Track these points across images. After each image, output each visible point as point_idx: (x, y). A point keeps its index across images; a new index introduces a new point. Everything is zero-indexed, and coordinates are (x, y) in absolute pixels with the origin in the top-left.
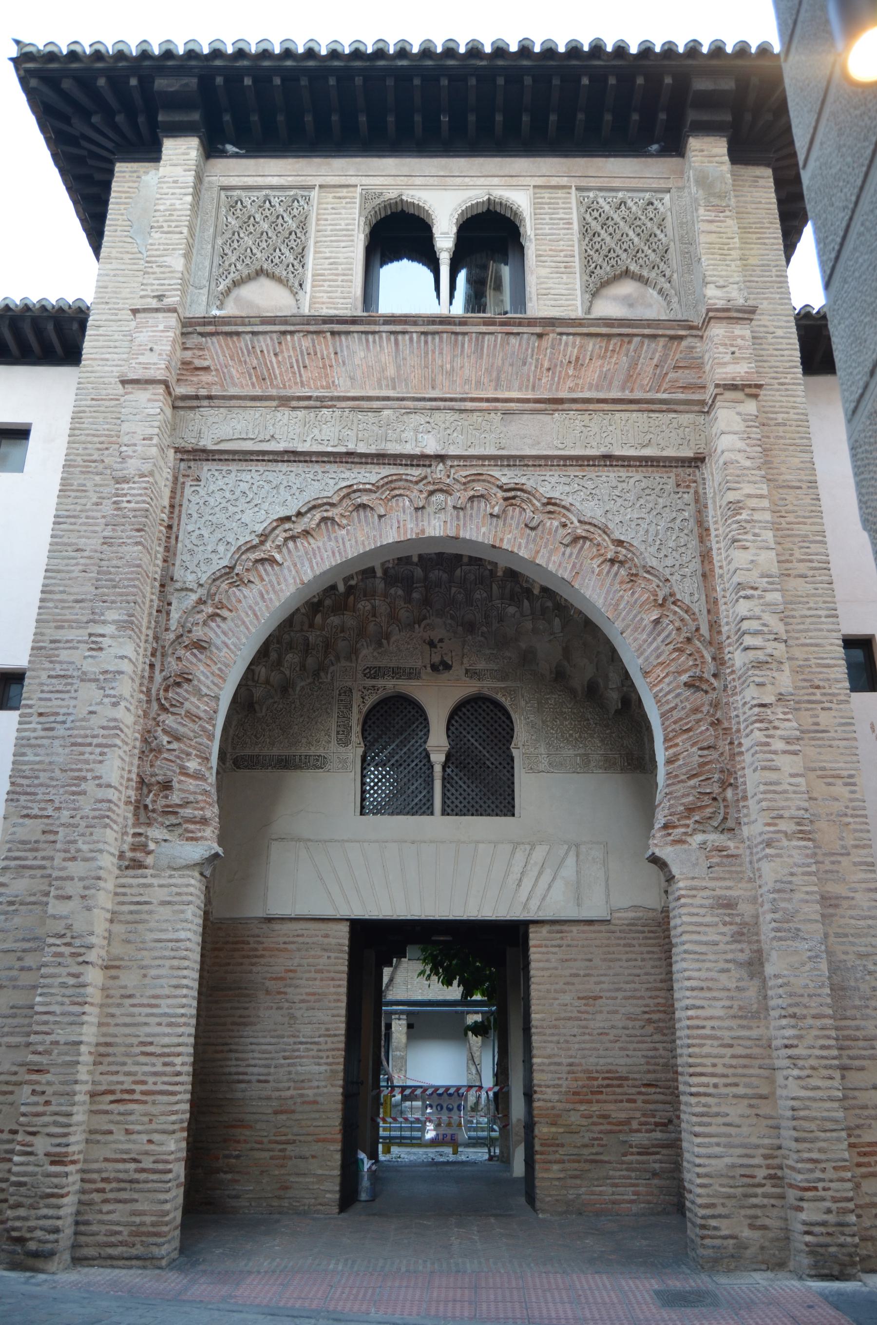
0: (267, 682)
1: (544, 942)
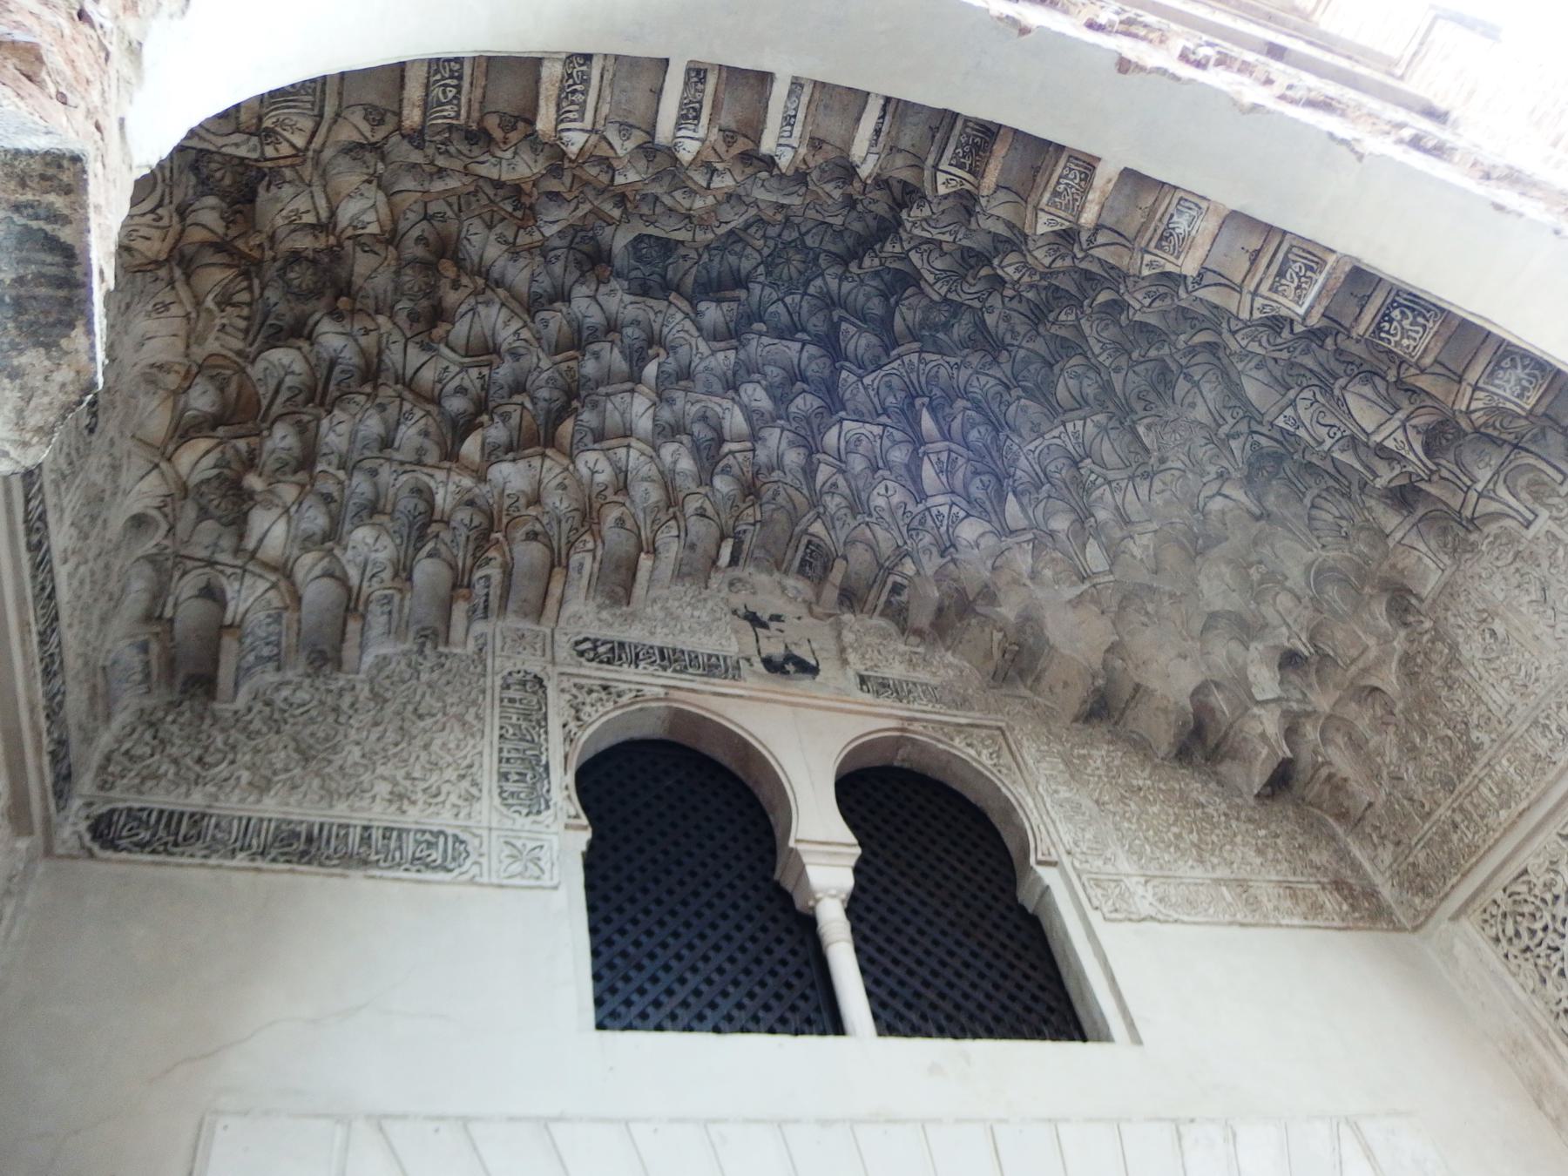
0: (284, 570)
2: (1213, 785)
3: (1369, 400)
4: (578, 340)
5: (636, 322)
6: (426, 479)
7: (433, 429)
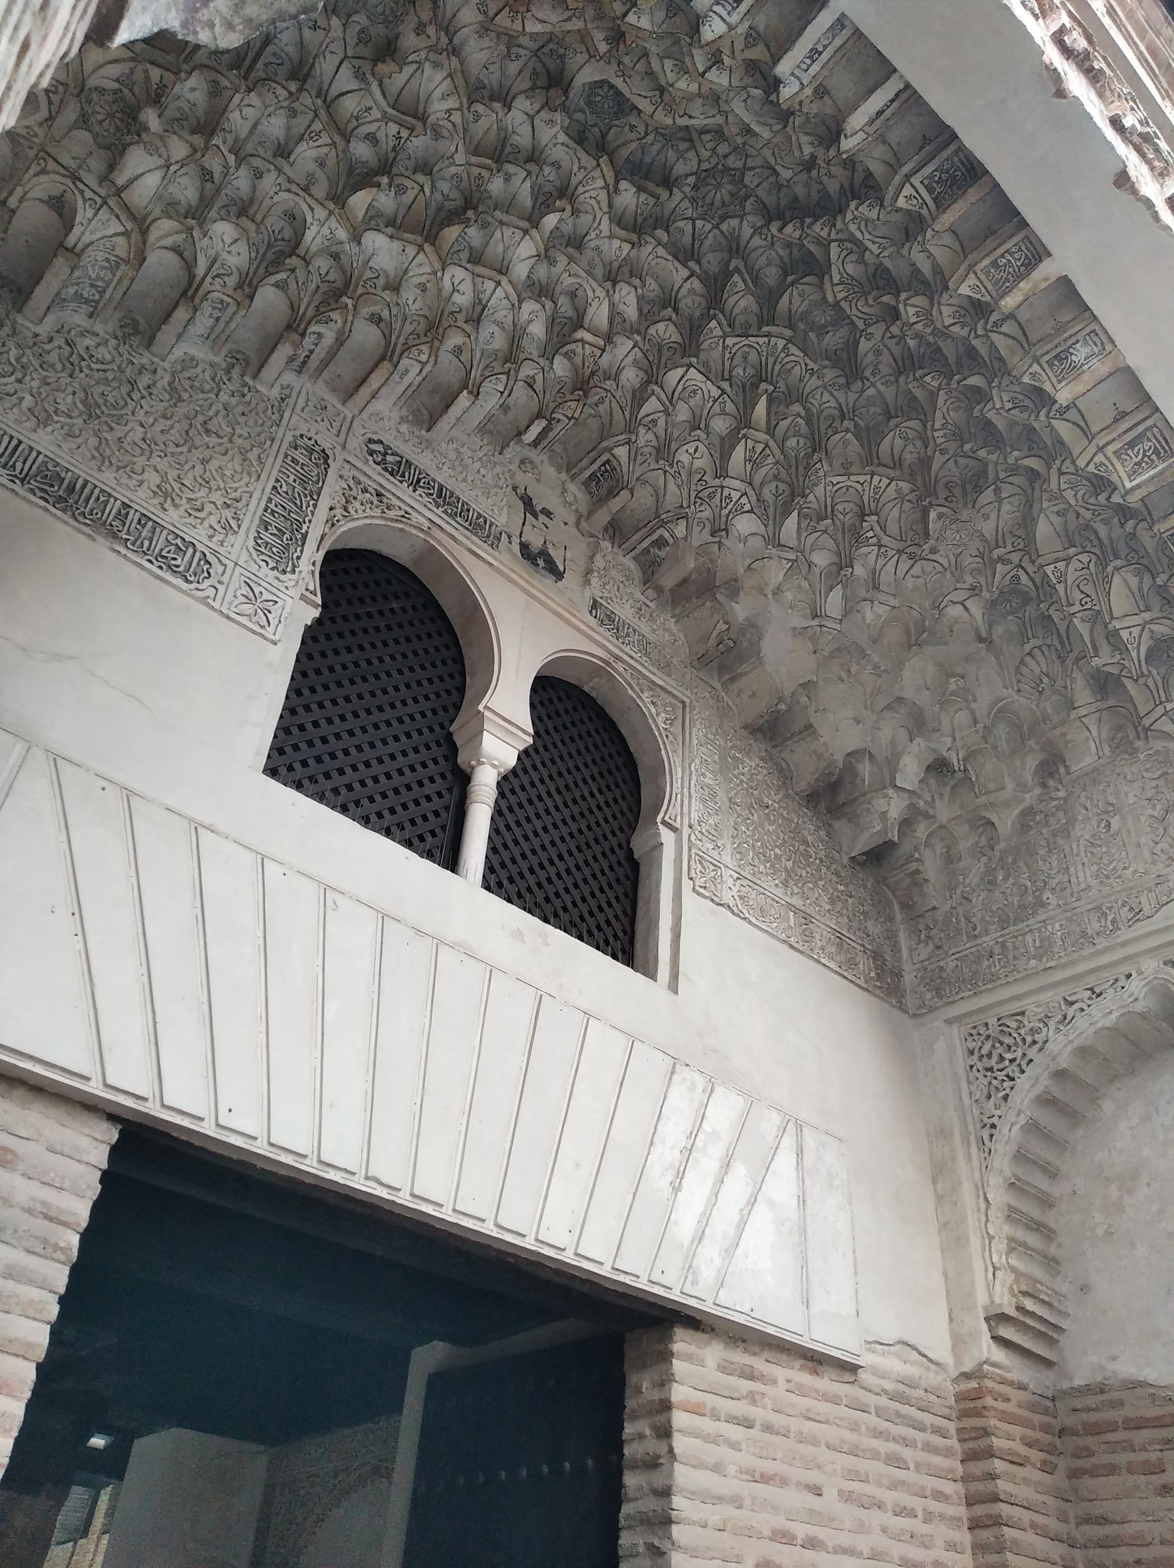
1: (711, 1400)
2: (822, 833)
3: (1130, 590)
4: (499, 153)
5: (556, 165)
6: (305, 208)
7: (331, 162)
